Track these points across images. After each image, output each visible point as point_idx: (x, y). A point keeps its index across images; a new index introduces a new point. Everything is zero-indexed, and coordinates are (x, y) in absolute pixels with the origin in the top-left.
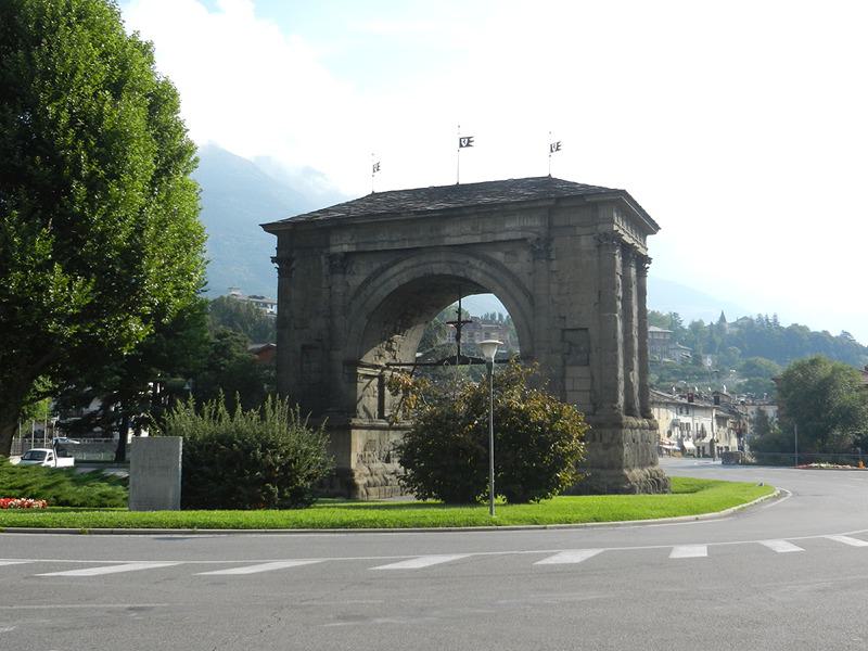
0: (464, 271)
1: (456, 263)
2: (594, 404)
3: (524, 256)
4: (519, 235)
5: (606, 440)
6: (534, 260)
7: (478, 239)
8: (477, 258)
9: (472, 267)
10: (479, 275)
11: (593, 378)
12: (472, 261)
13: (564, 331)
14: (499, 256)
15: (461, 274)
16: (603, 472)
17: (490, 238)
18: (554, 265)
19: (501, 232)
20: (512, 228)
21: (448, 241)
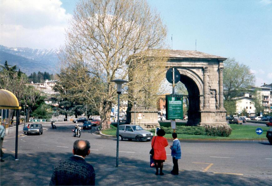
0: (185, 73)
1: (183, 71)
2: (216, 107)
3: (201, 70)
4: (201, 66)
5: (222, 115)
6: (204, 73)
7: (190, 66)
8: (189, 70)
9: (188, 73)
10: (190, 75)
11: (216, 101)
12: (188, 71)
13: (211, 90)
14: (194, 70)
15: (185, 74)
16: (222, 123)
17: (193, 66)
18: (208, 74)
19: (196, 65)
20: (199, 64)
21: (183, 66)
